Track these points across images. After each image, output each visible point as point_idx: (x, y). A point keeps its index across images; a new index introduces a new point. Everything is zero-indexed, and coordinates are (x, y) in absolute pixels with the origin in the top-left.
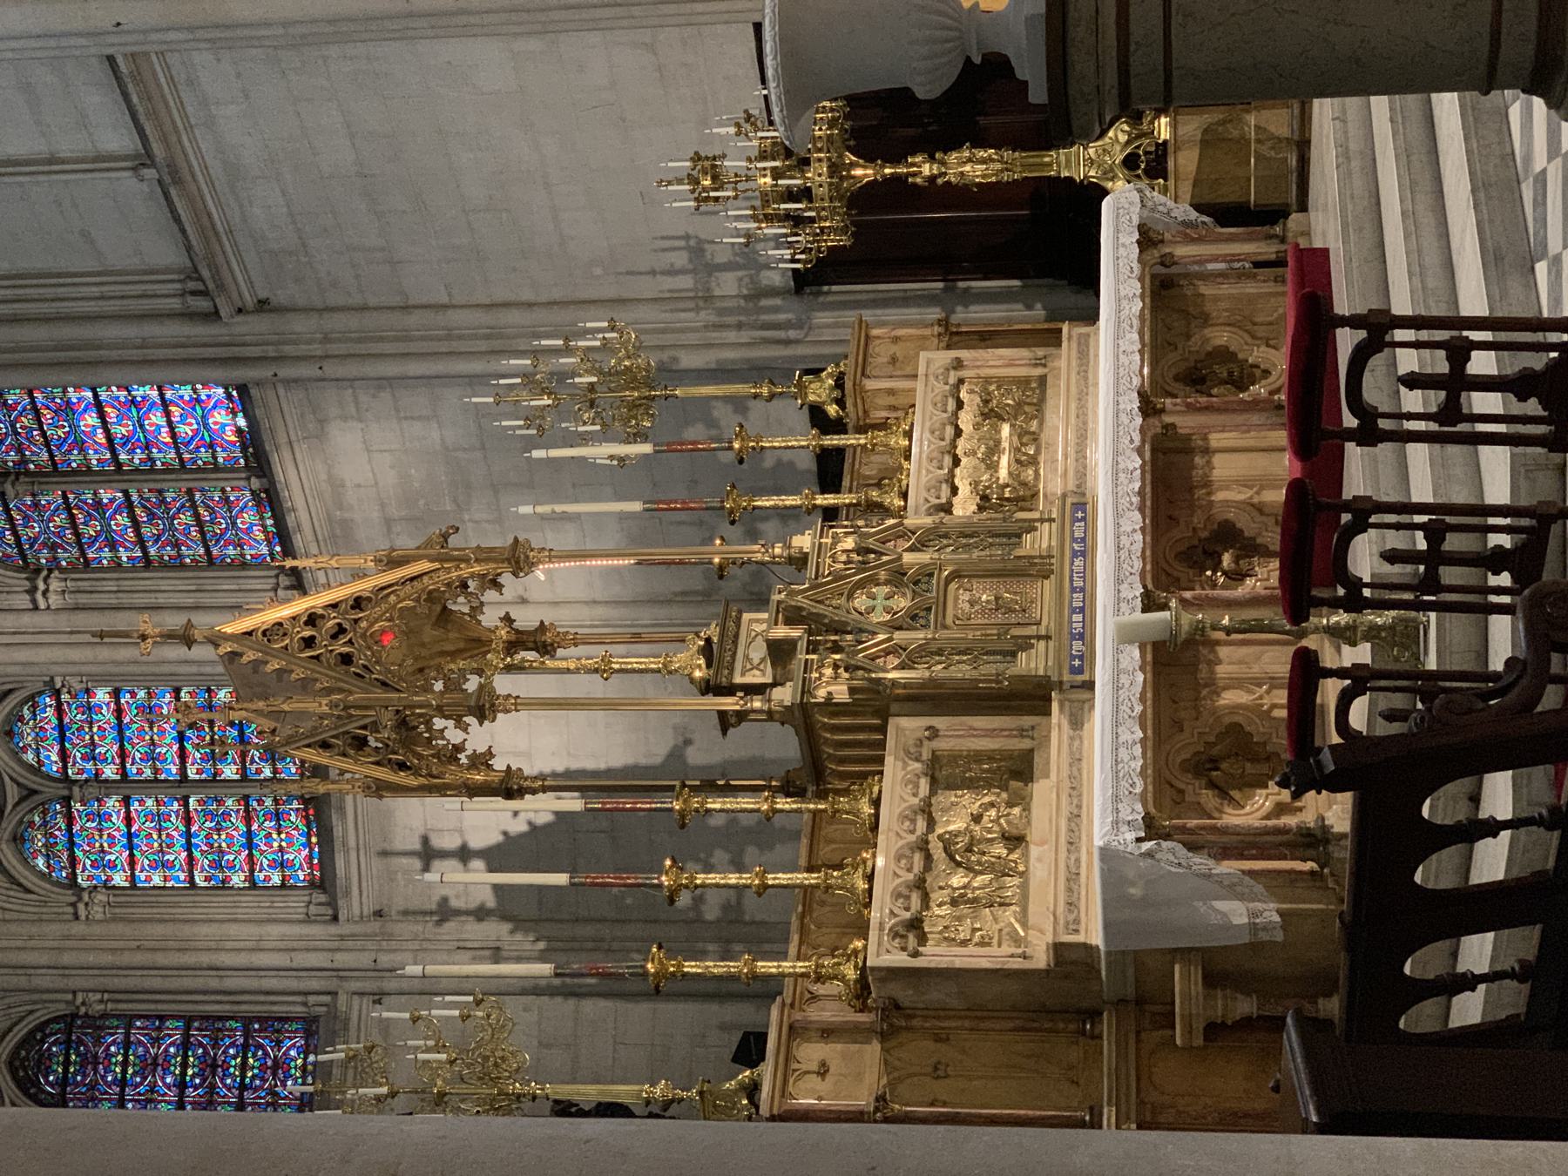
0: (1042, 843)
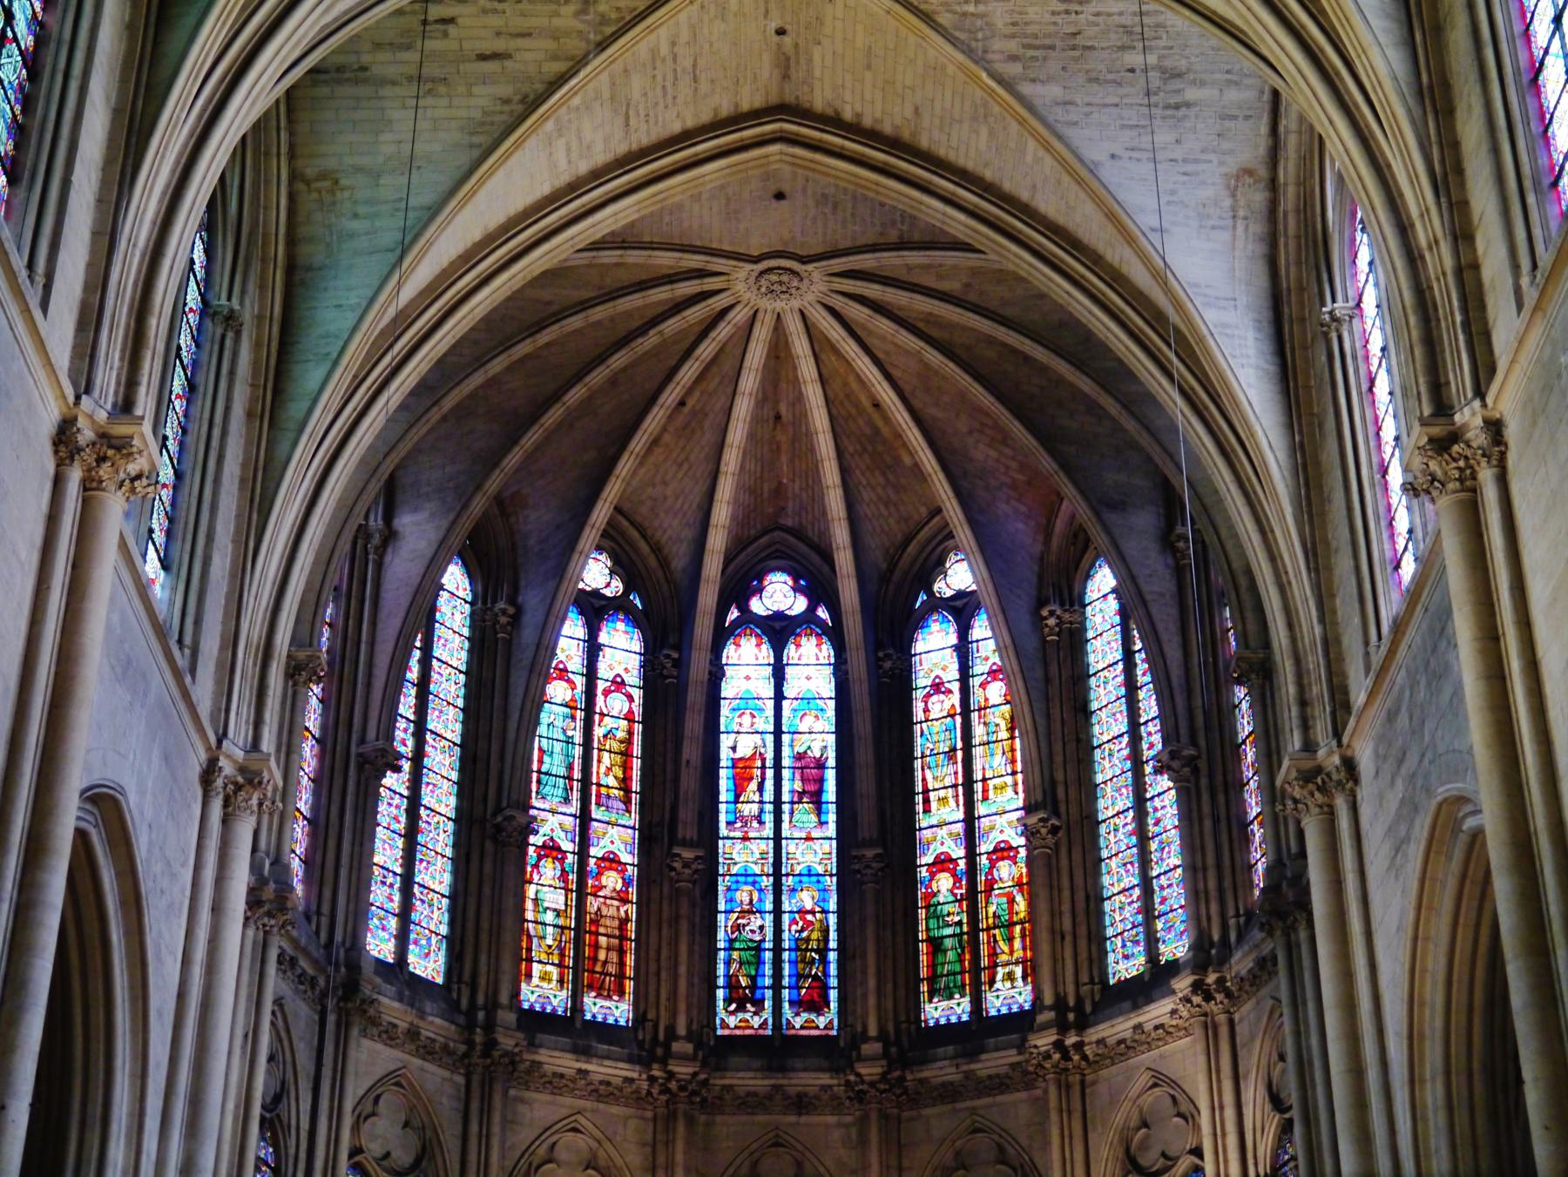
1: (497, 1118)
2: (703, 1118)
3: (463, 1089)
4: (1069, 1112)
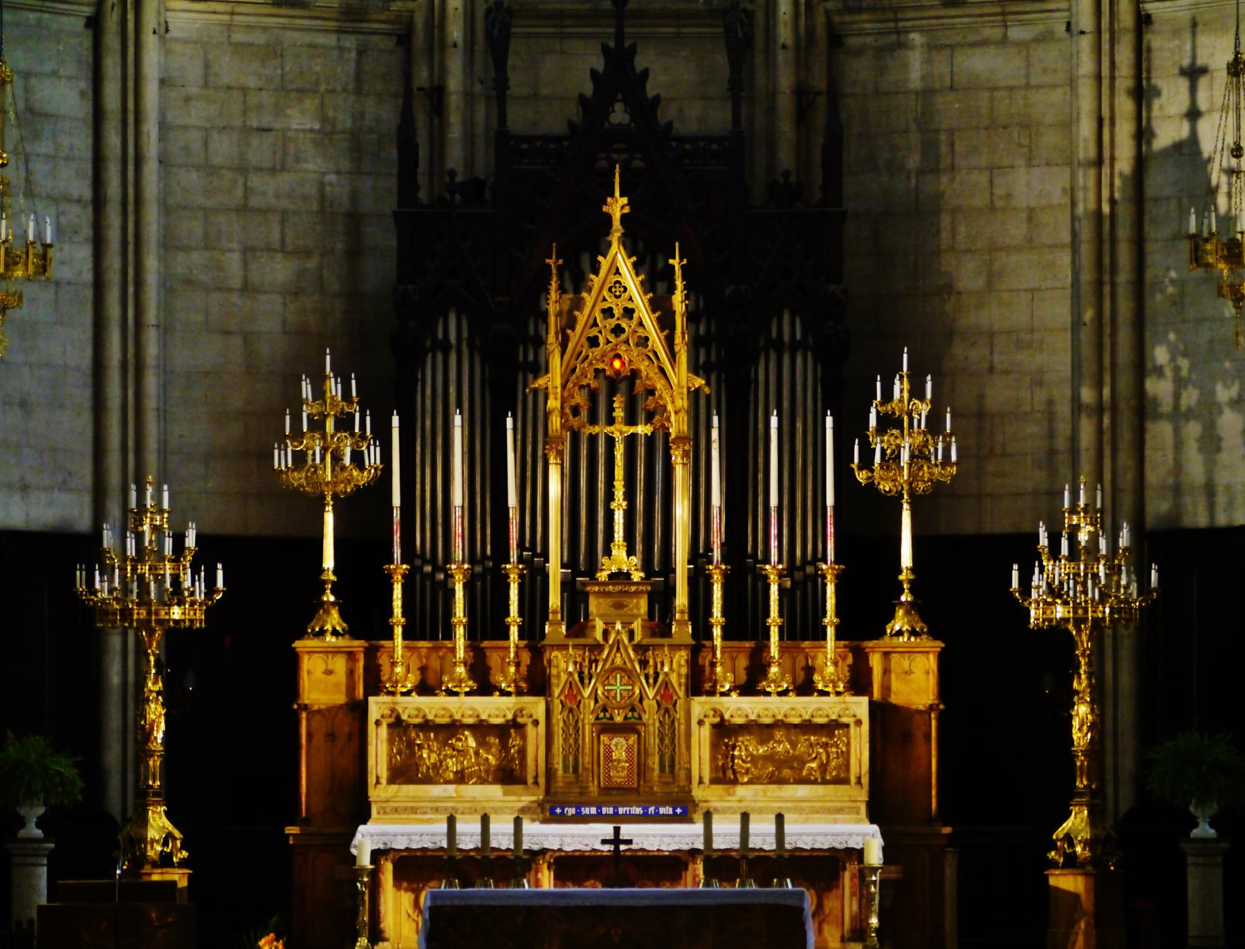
0: (456, 791)
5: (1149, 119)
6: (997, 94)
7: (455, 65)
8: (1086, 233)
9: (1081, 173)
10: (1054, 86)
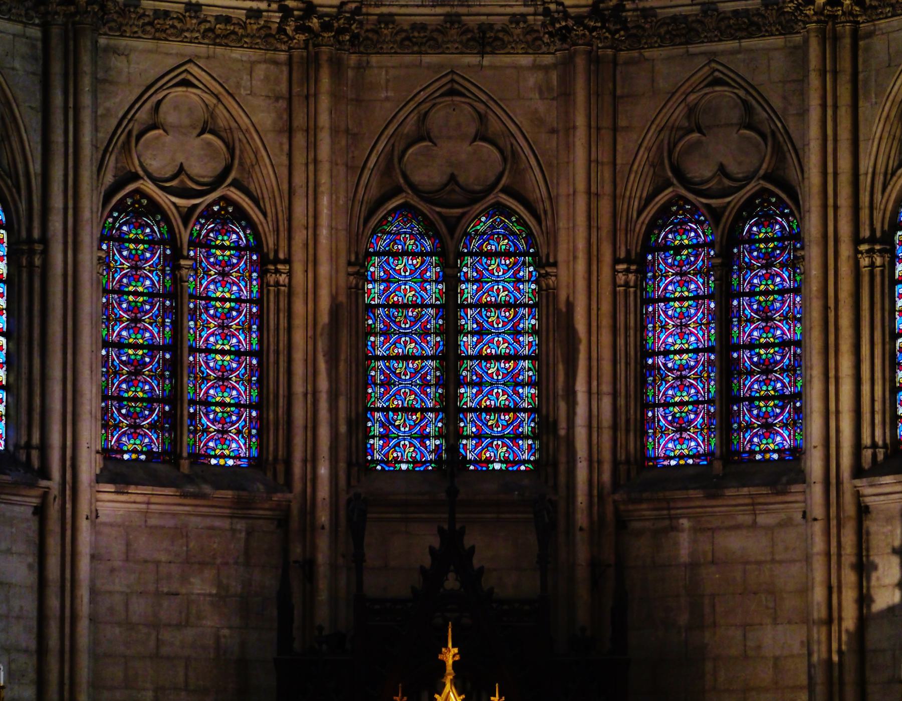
1: (86, 83)
2: (353, 59)
3: (39, 44)
4: (835, 73)
5: (868, 588)
6: (748, 567)
7: (323, 543)
8: (820, 676)
9: (815, 630)
10: (793, 561)
